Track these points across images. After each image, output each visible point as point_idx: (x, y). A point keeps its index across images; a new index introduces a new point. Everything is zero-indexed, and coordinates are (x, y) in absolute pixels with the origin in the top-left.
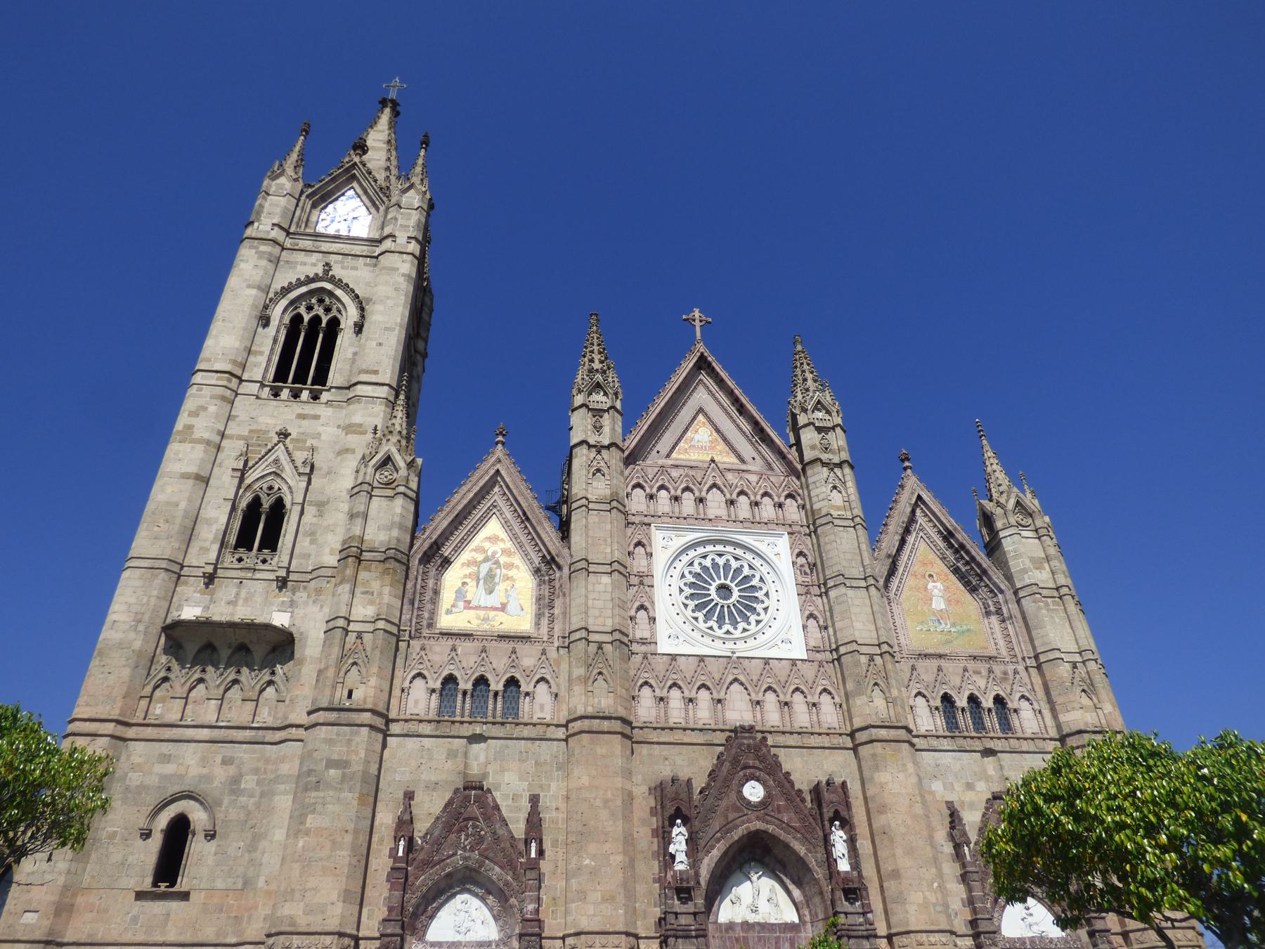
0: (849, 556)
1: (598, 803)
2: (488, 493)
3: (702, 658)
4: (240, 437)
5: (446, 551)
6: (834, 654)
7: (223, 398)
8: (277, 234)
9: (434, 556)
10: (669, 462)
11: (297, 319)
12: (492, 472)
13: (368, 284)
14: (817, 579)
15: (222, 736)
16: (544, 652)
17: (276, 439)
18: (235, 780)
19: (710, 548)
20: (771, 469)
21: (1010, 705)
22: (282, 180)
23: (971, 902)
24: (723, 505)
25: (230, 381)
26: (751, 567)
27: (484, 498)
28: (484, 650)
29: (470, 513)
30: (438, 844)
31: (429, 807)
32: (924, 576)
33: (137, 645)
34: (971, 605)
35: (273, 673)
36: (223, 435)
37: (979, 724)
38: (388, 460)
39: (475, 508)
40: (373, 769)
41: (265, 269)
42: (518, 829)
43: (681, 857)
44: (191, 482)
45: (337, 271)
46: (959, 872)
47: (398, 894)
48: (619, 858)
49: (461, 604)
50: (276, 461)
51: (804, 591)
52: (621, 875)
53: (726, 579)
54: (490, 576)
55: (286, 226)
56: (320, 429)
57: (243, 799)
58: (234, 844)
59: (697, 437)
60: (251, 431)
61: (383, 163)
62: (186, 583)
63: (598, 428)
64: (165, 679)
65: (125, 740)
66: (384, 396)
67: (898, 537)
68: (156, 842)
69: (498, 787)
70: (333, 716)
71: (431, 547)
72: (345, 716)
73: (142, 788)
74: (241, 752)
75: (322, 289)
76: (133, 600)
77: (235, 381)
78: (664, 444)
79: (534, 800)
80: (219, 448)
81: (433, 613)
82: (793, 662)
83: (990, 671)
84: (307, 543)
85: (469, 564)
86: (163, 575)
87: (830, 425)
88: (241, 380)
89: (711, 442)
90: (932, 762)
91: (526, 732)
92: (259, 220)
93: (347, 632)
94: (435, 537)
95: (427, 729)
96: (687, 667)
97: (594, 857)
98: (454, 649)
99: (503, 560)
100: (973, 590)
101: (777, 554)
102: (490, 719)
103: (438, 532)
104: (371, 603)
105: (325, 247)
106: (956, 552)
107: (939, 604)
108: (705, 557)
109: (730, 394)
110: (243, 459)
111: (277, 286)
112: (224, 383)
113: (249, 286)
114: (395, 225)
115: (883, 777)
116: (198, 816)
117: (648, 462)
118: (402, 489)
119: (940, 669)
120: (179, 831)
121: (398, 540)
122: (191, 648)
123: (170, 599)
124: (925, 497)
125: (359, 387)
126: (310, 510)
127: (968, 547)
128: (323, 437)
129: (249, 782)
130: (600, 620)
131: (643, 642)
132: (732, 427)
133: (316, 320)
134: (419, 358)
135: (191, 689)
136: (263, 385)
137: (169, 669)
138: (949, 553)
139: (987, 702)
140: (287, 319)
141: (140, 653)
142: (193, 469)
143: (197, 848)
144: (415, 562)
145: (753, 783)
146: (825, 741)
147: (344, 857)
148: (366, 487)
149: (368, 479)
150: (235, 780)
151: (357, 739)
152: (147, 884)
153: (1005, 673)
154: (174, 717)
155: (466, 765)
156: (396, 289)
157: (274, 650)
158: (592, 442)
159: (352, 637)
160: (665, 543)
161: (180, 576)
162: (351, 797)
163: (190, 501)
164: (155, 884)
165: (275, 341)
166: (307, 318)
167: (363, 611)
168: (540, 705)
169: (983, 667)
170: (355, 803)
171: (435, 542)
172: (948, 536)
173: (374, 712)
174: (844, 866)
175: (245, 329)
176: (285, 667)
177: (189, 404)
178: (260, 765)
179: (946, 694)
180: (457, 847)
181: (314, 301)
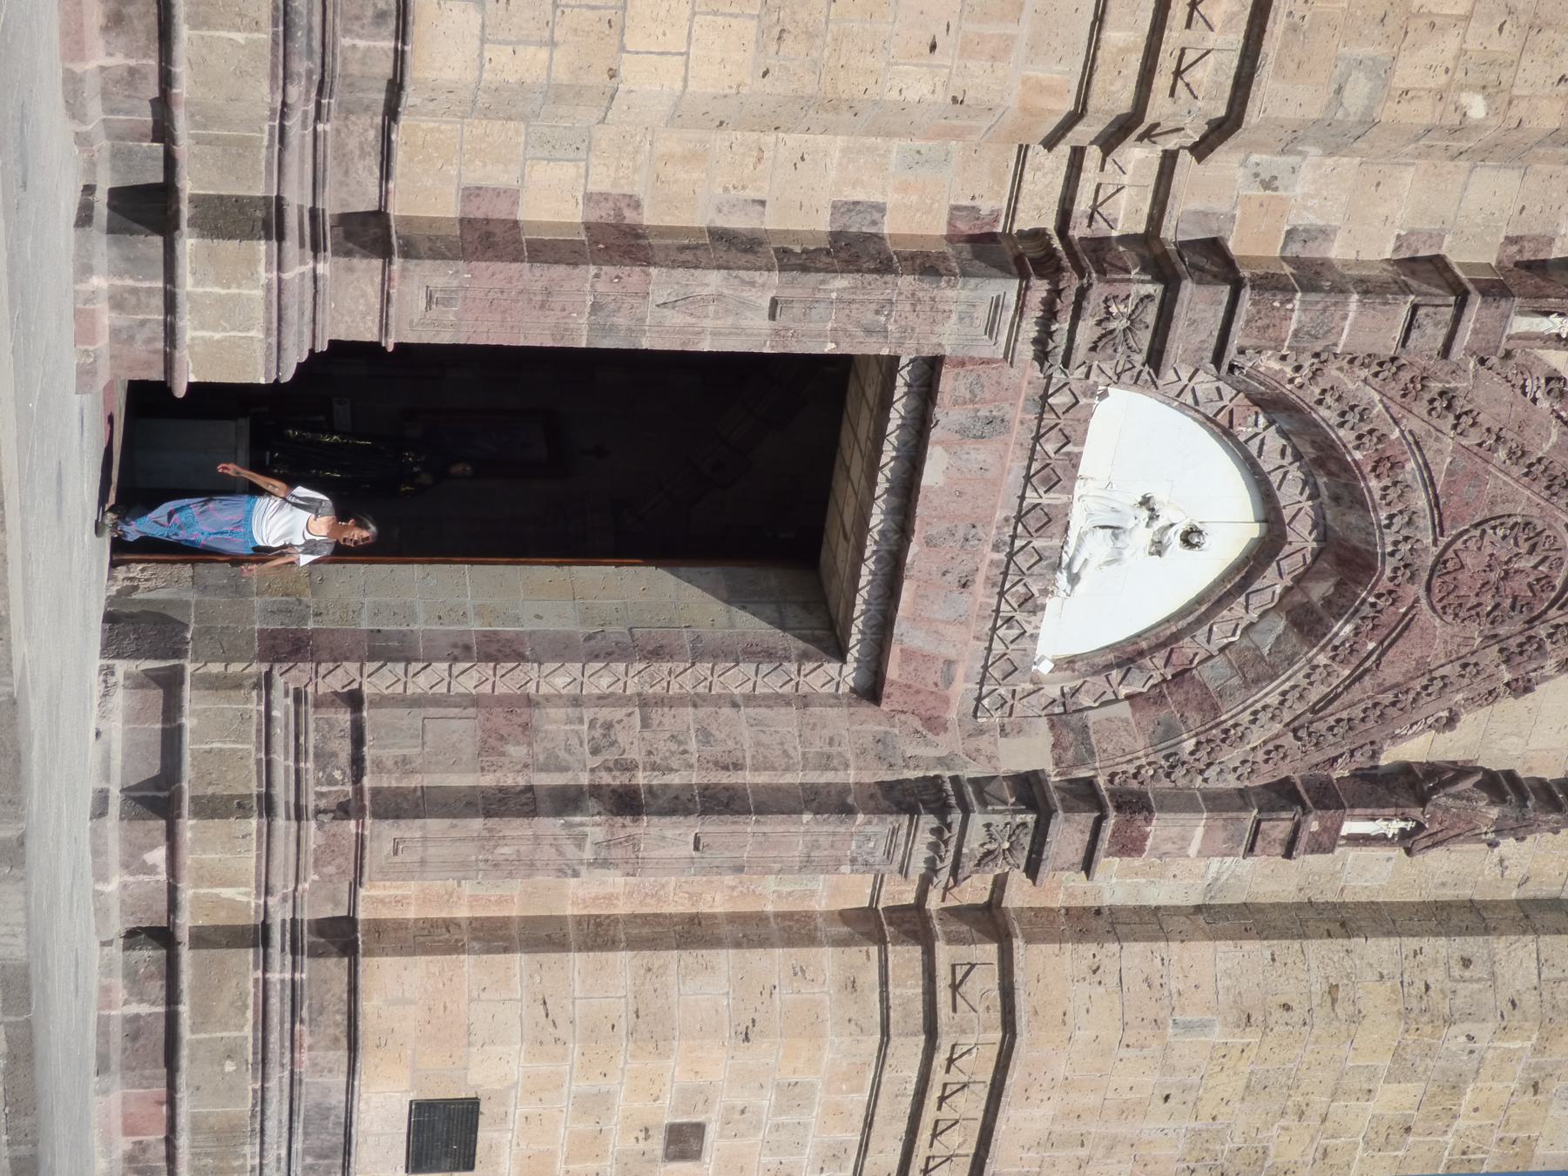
23: (1311, 276)
46: (1459, 255)
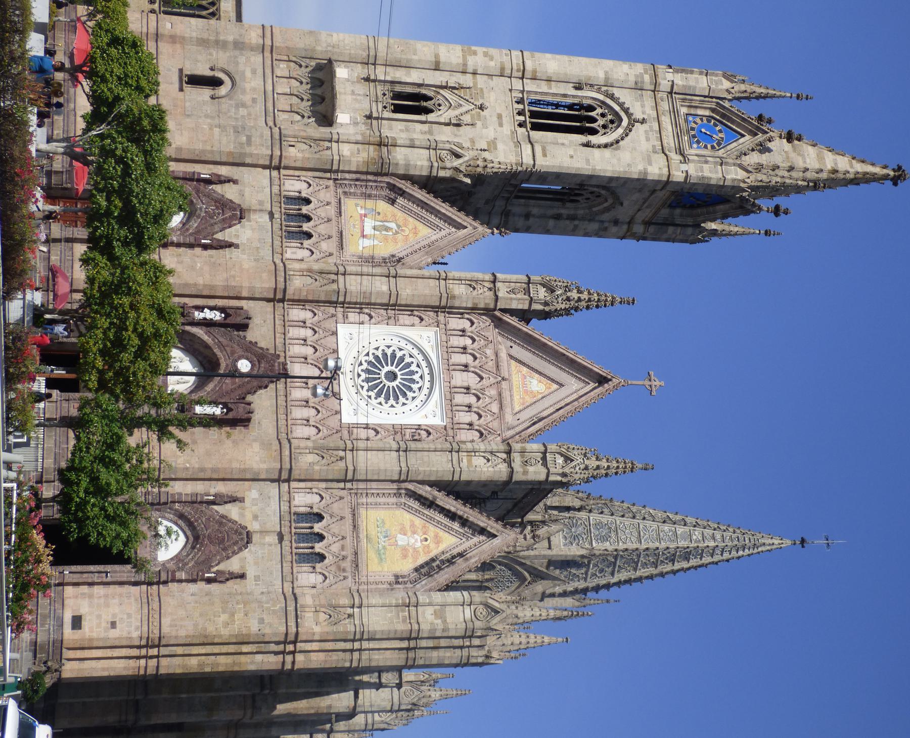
0: (426, 459)
1: (233, 273)
2: (449, 224)
3: (336, 351)
4: (475, 84)
5: (400, 200)
6: (347, 440)
7: (503, 69)
8: (665, 85)
9: (395, 193)
10: (503, 355)
11: (591, 108)
12: (465, 224)
13: (634, 149)
14: (408, 439)
15: (269, 98)
16: (331, 255)
17: (478, 103)
18: (244, 105)
19: (426, 371)
20: (509, 429)
21: (318, 566)
22: (727, 84)
24: (465, 384)
25: (518, 70)
26: (414, 398)
27: (445, 221)
28: (329, 220)
29: (431, 213)
30: (208, 196)
31: (229, 192)
32: (425, 533)
33: (319, 48)
34: (406, 566)
35: (309, 117)
36: (475, 73)
37: (302, 538)
38: (458, 156)
39: (436, 216)
40: (248, 160)
41: (626, 81)
42: (219, 236)
43: (202, 315)
44: (433, 59)
45: (639, 128)
47: (181, 175)
48: (201, 282)
49: (363, 212)
50: (461, 105)
51: (397, 430)
52: (192, 282)
53: (402, 375)
54: (387, 229)
55: (675, 89)
56: (491, 128)
57: (233, 110)
58: (210, 108)
59: (535, 382)
60: (482, 89)
61: (800, 163)
62: (363, 68)
63: (513, 291)
64: (301, 66)
65: (263, 52)
66: (525, 161)
67: (453, 509)
68: (209, 73)
69: (243, 227)
70: (277, 136)
71: (400, 189)
72: (278, 142)
73: (237, 63)
74: (260, 107)
75: (621, 120)
76: (346, 42)
77: (520, 74)
78: (518, 351)
79: (237, 246)
80: (464, 72)
81: (354, 194)
82: (338, 412)
83: (344, 558)
84: (400, 128)
85: (394, 216)
86: (365, 54)
87: (550, 464)
88: (522, 78)
89: (532, 392)
90: (271, 494)
91: (277, 243)
92: (677, 71)
93: (330, 141)
94: (407, 190)
95: (276, 189)
96: (330, 341)
97: (201, 269)
98: (328, 204)
99: (399, 237)
100: (416, 570)
101: (424, 411)
102: (284, 223)
103: (411, 192)
104: (352, 154)
105: (666, 121)
106: (448, 561)
107: (402, 540)
108: (418, 366)
109: (576, 400)
110: (457, 86)
111: (617, 93)
112: (515, 67)
113: (606, 73)
114: (699, 162)
115: (256, 447)
116: (223, 90)
117: (500, 338)
118: (435, 164)
119: (342, 518)
120: (215, 82)
121: (397, 164)
122: (319, 75)
123: (350, 62)
124: (496, 541)
125: (529, 146)
126: (426, 127)
127: (452, 567)
128: (484, 130)
129: (243, 112)
130: (353, 283)
131: (345, 317)
132: (547, 406)
133: (594, 120)
134: (625, 227)
135: (295, 79)
136: (522, 92)
137: (307, 67)
138: (448, 556)
139: (319, 547)
140: (586, 102)
141: (314, 50)
142: (442, 59)
143: (205, 93)
144: (386, 179)
145: (250, 365)
146: (282, 423)
147: (199, 146)
148: (433, 145)
149: (440, 146)
150: (244, 105)
151: (264, 149)
152: (187, 72)
153: (344, 570)
154: (278, 72)
155: (255, 211)
156: (629, 165)
157: (325, 116)
158: (498, 285)
159: (329, 144)
160: (424, 337)
161: (367, 64)
162: (231, 148)
163: (419, 61)
164: (186, 75)
165: (565, 96)
166: (593, 114)
167: (346, 150)
168: (294, 252)
169: (349, 552)
170: (228, 150)
171: (404, 192)
172: (461, 555)
173: (281, 156)
174: (198, 409)
175: (566, 74)
176: (314, 123)
177: (493, 51)
178: (253, 116)
179: (323, 518)
180: (208, 204)
181: (610, 117)
